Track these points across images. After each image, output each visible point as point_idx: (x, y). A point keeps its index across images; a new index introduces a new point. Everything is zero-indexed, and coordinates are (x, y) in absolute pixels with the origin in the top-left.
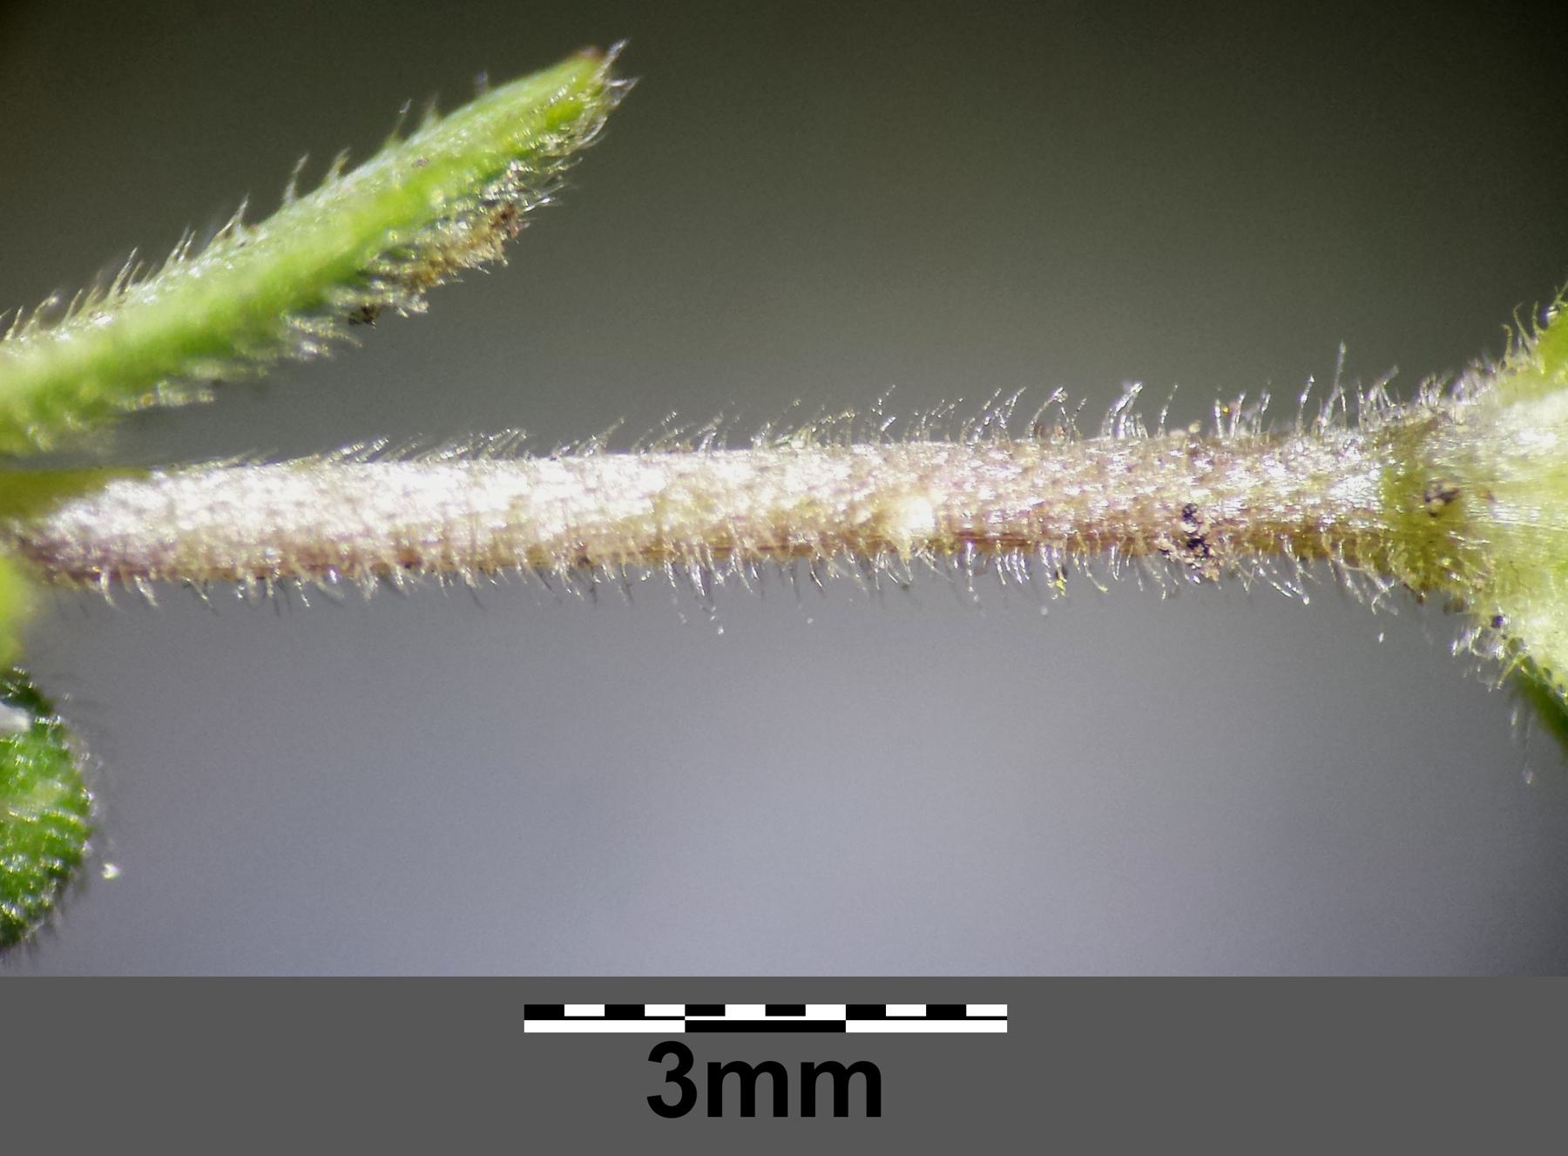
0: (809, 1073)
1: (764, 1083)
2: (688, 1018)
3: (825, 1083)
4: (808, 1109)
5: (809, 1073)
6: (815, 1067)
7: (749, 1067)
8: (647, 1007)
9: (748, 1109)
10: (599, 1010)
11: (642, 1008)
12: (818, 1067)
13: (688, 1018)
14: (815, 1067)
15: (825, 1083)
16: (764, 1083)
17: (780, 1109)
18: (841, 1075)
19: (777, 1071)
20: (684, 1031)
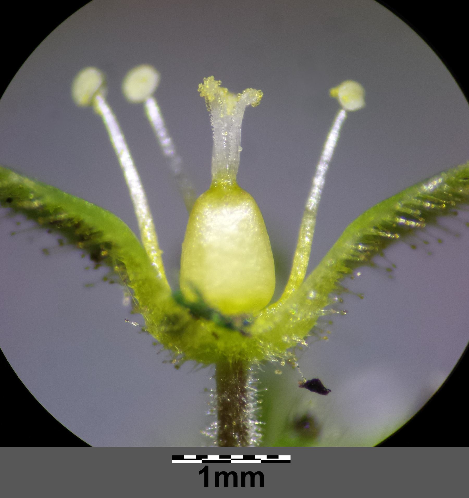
0: (244, 475)
1: (231, 478)
2: (230, 459)
3: (248, 478)
4: (243, 485)
5: (244, 475)
6: (219, 473)
7: (253, 473)
8: (255, 456)
9: (226, 485)
10: (242, 457)
11: (254, 456)
12: (246, 473)
13: (230, 459)
14: (245, 473)
15: (248, 478)
16: (231, 478)
17: (235, 485)
18: (226, 475)
19: (235, 474)
20: (260, 463)
